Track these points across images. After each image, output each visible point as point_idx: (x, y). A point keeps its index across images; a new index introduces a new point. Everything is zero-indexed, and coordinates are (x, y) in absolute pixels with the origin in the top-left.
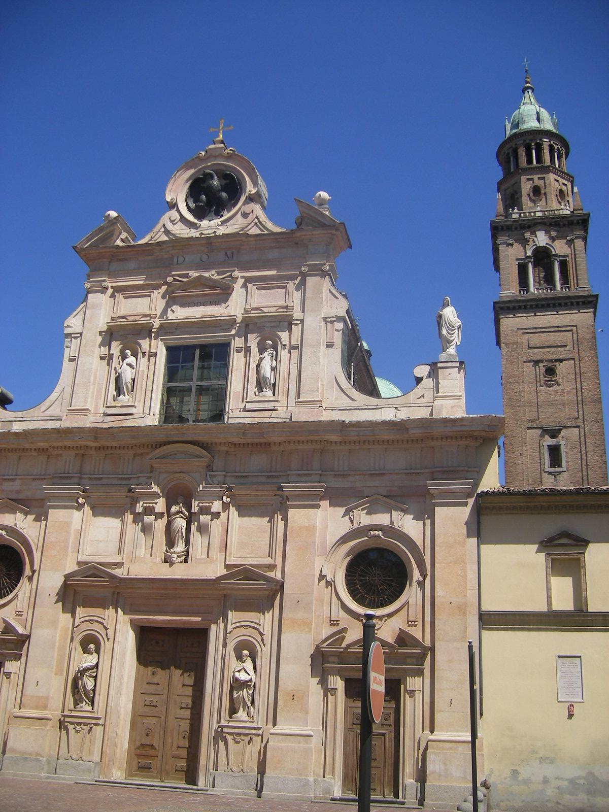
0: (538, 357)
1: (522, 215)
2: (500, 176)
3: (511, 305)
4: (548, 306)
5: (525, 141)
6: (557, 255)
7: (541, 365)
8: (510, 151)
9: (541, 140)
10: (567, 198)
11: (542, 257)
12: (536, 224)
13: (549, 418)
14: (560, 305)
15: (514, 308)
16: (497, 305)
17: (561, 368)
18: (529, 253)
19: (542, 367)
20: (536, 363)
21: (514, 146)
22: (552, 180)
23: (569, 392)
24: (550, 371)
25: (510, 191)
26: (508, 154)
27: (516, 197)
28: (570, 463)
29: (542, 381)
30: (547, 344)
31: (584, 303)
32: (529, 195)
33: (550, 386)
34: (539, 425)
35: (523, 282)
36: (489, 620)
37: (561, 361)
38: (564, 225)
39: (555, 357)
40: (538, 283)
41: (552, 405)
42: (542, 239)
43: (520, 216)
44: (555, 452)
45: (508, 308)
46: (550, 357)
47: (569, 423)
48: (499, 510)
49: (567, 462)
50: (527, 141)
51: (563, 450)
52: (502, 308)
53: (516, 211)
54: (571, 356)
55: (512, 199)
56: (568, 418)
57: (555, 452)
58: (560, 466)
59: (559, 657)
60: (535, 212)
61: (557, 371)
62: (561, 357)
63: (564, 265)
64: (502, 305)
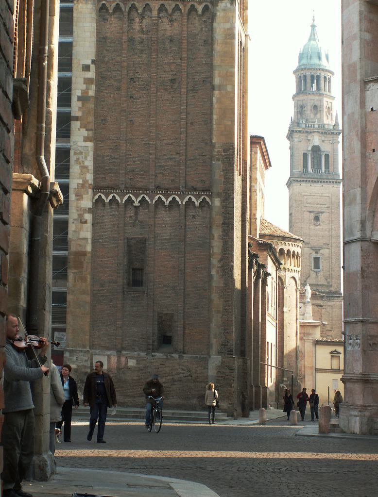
0: (311, 210)
1: (307, 125)
2: (294, 92)
3: (299, 179)
4: (318, 182)
5: (311, 73)
6: (324, 152)
7: (312, 214)
8: (302, 76)
9: (320, 74)
10: (331, 112)
11: (316, 150)
12: (314, 132)
13: (315, 242)
14: (324, 182)
15: (300, 181)
16: (292, 179)
17: (322, 217)
18: (310, 148)
19: (313, 215)
20: (310, 212)
21: (304, 74)
22: (324, 101)
23: (325, 230)
24: (317, 218)
25: (300, 103)
26: (300, 77)
27: (304, 109)
28: (324, 267)
29: (312, 224)
30: (316, 202)
31: (336, 182)
32: (311, 110)
33: (317, 226)
34: (310, 246)
35: (305, 166)
36: (317, 370)
37: (322, 213)
38: (329, 134)
39: (319, 210)
40: (313, 166)
41: (317, 236)
42: (316, 140)
43: (306, 126)
44: (317, 260)
45: (297, 181)
46: (316, 210)
47: (324, 247)
48: (320, 344)
49: (322, 266)
50: (312, 74)
51: (321, 260)
52: (294, 180)
53: (304, 122)
54: (327, 211)
55: (300, 110)
56: (324, 244)
57: (317, 260)
58: (318, 268)
59: (333, 380)
60: (314, 125)
61: (320, 219)
62: (322, 211)
63: (327, 156)
64: (294, 179)
